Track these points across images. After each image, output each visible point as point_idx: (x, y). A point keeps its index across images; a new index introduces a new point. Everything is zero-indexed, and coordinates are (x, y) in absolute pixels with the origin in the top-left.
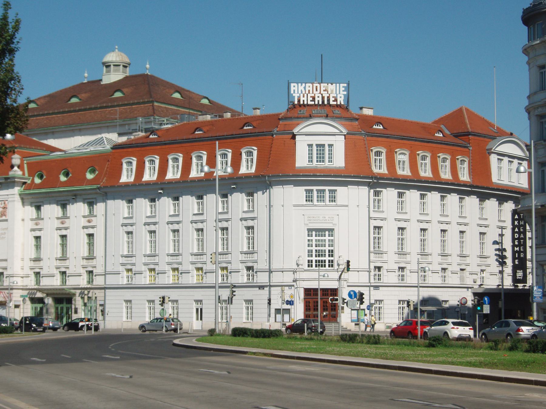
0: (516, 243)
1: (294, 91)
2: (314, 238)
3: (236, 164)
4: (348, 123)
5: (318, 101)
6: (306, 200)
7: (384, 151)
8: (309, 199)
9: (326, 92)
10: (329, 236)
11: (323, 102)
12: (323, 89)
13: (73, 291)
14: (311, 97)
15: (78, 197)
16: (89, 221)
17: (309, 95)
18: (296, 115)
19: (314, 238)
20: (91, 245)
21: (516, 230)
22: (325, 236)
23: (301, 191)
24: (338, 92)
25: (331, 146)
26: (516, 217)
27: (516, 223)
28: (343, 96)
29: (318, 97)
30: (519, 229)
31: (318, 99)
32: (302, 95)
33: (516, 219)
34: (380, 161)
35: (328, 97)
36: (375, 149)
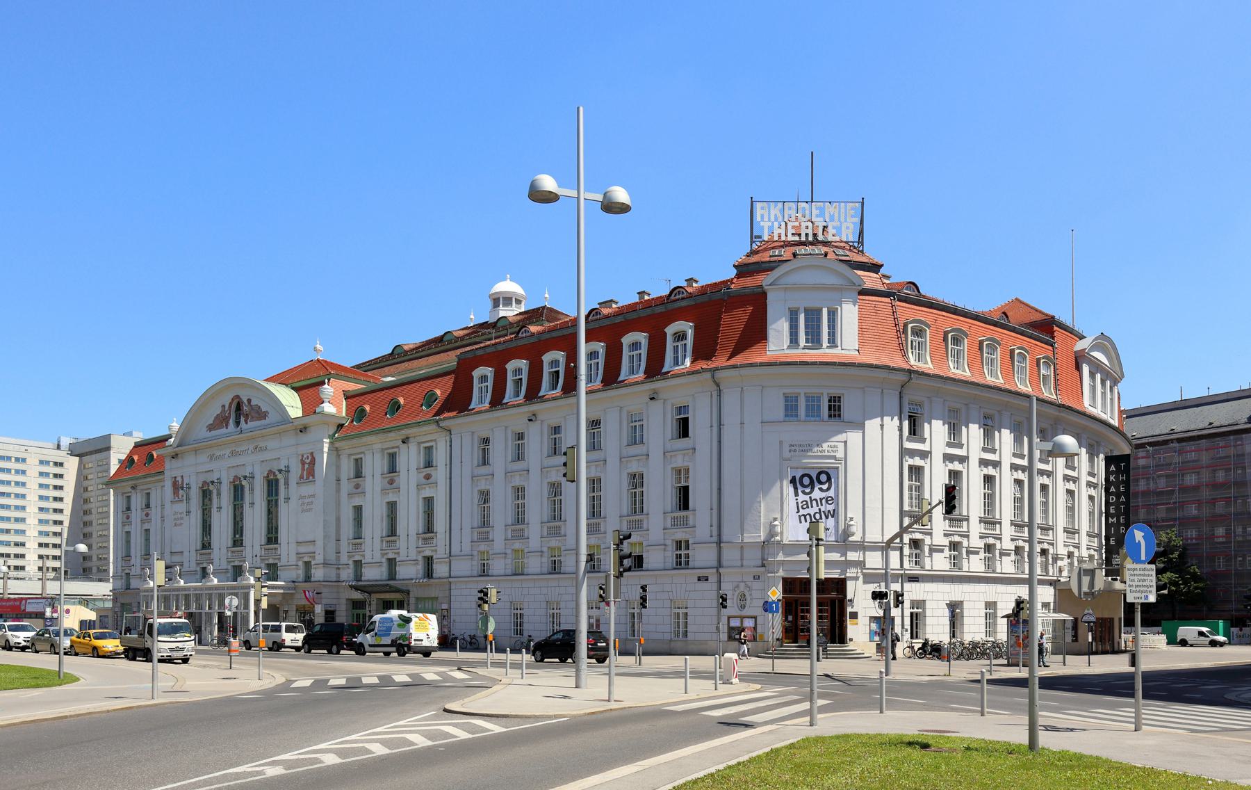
0: (1112, 511)
1: (762, 216)
5: (807, 235)
8: (790, 408)
11: (815, 235)
12: (815, 212)
17: (790, 225)
21: (1113, 489)
26: (1113, 468)
27: (1112, 478)
28: (852, 226)
30: (1117, 488)
32: (776, 224)
33: (1112, 473)
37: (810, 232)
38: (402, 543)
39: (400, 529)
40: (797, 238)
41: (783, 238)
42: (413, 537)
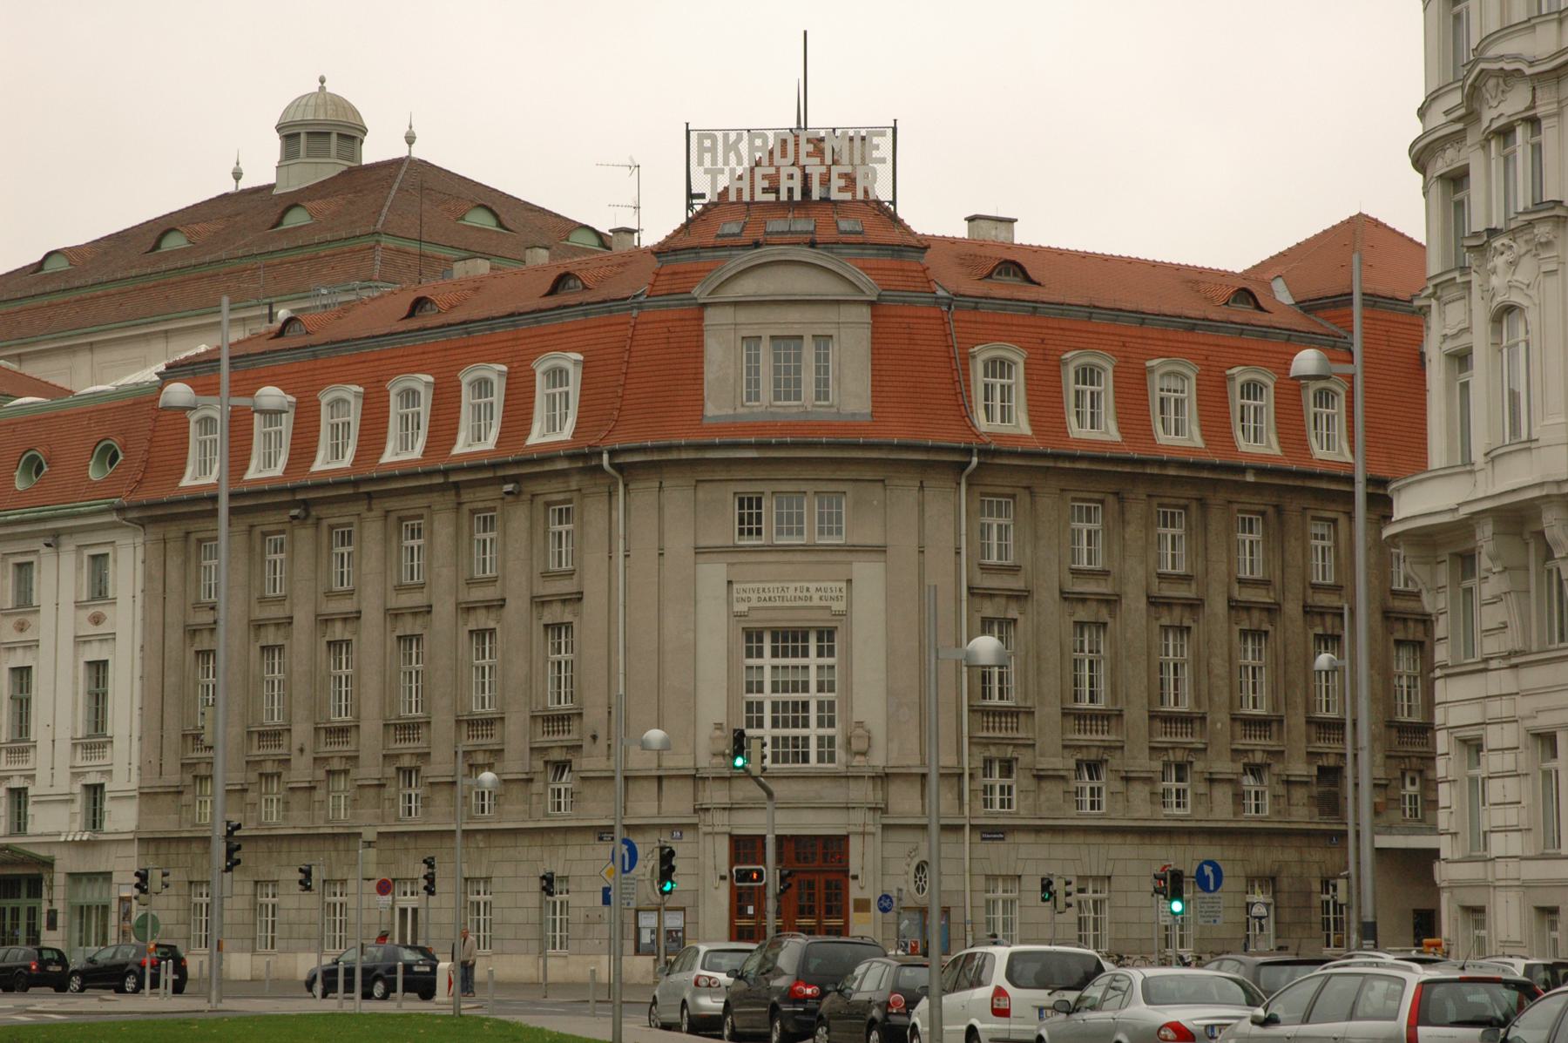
2: (767, 661)
3: (518, 414)
4: (886, 261)
5: (790, 190)
6: (741, 532)
7: (1018, 357)
8: (750, 522)
9: (817, 160)
10: (820, 654)
11: (806, 191)
13: (43, 853)
14: (764, 177)
15: (64, 539)
16: (97, 620)
18: (711, 241)
19: (767, 661)
20: (98, 700)
22: (805, 654)
23: (723, 500)
24: (857, 160)
25: (823, 340)
29: (791, 177)
31: (791, 184)
34: (1006, 391)
35: (825, 181)
36: (983, 354)
37: (797, 185)
38: (39, 760)
39: (38, 731)
40: (771, 197)
41: (746, 198)
42: (64, 746)
